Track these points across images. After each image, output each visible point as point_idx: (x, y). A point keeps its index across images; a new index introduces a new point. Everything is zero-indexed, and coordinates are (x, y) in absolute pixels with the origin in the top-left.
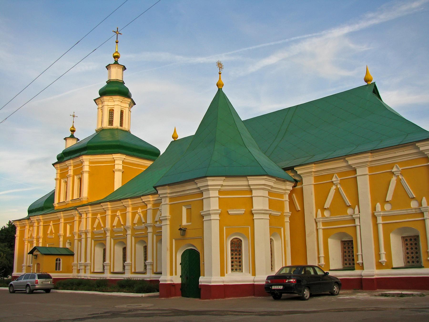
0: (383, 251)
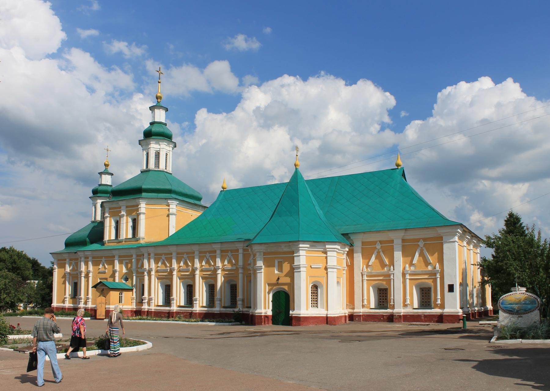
0: (408, 297)
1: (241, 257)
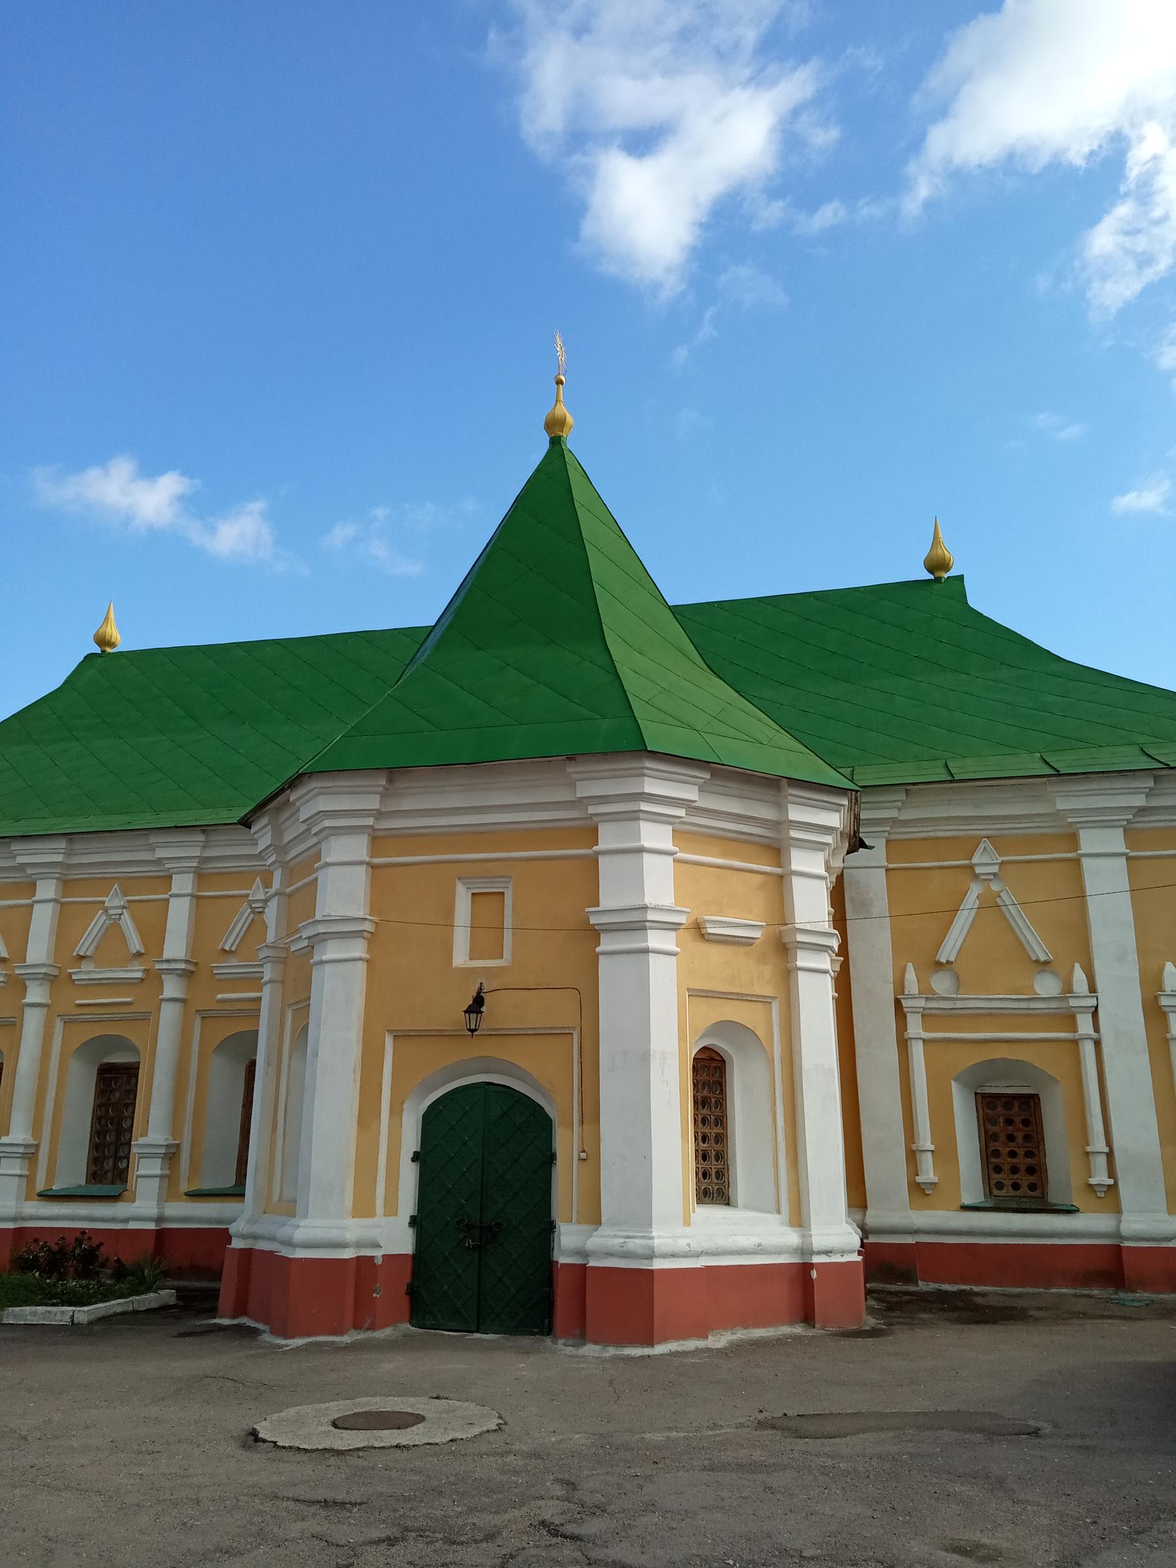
1: (179, 915)
